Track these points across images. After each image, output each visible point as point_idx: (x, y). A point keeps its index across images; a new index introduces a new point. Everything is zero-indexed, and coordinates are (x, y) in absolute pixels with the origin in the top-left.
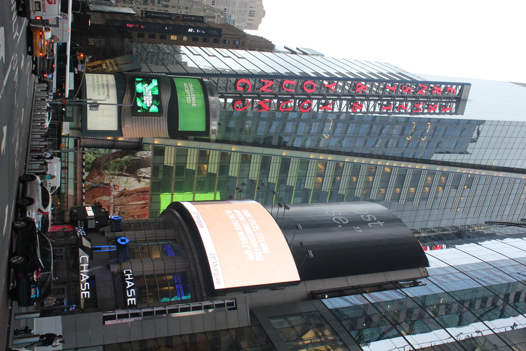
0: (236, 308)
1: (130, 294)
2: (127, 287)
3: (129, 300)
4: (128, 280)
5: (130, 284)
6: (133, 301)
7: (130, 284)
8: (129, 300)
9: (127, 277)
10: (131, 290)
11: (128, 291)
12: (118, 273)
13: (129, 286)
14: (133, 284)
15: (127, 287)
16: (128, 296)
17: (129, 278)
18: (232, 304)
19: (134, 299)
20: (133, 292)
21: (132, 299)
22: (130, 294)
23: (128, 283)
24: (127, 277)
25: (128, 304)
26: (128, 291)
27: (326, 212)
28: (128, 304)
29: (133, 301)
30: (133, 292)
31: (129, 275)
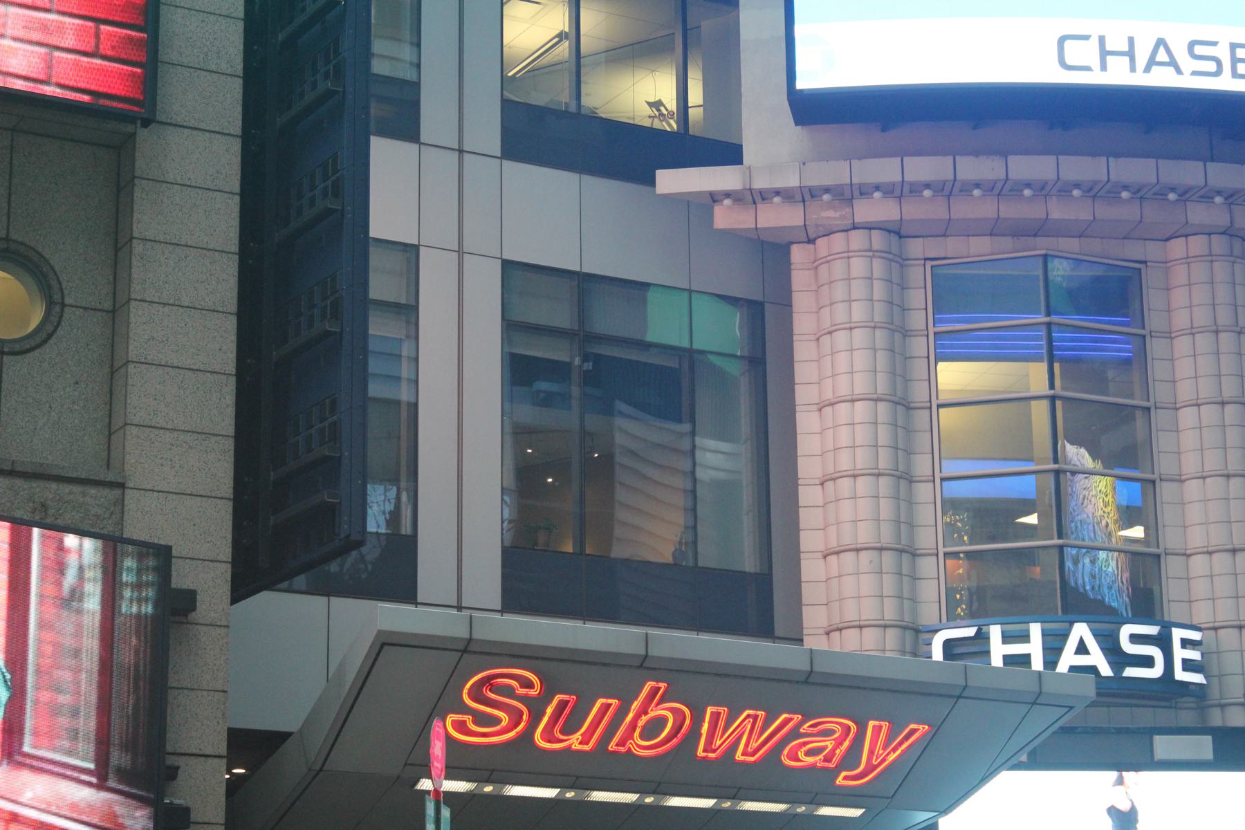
1: (1148, 662)
2: (1106, 670)
3: (1180, 675)
4: (1051, 663)
5: (1082, 649)
6: (1185, 643)
7: (1082, 649)
11: (1131, 672)
13: (1097, 658)
15: (1106, 670)
16: (1157, 672)
17: (1034, 648)
19: (1178, 634)
20: (1135, 639)
21: (1179, 654)
22: (1148, 662)
23: (1068, 659)
25: (1197, 678)
26: (1131, 672)
28: (1197, 678)
29: (1185, 643)
30: (1135, 639)
31: (999, 650)
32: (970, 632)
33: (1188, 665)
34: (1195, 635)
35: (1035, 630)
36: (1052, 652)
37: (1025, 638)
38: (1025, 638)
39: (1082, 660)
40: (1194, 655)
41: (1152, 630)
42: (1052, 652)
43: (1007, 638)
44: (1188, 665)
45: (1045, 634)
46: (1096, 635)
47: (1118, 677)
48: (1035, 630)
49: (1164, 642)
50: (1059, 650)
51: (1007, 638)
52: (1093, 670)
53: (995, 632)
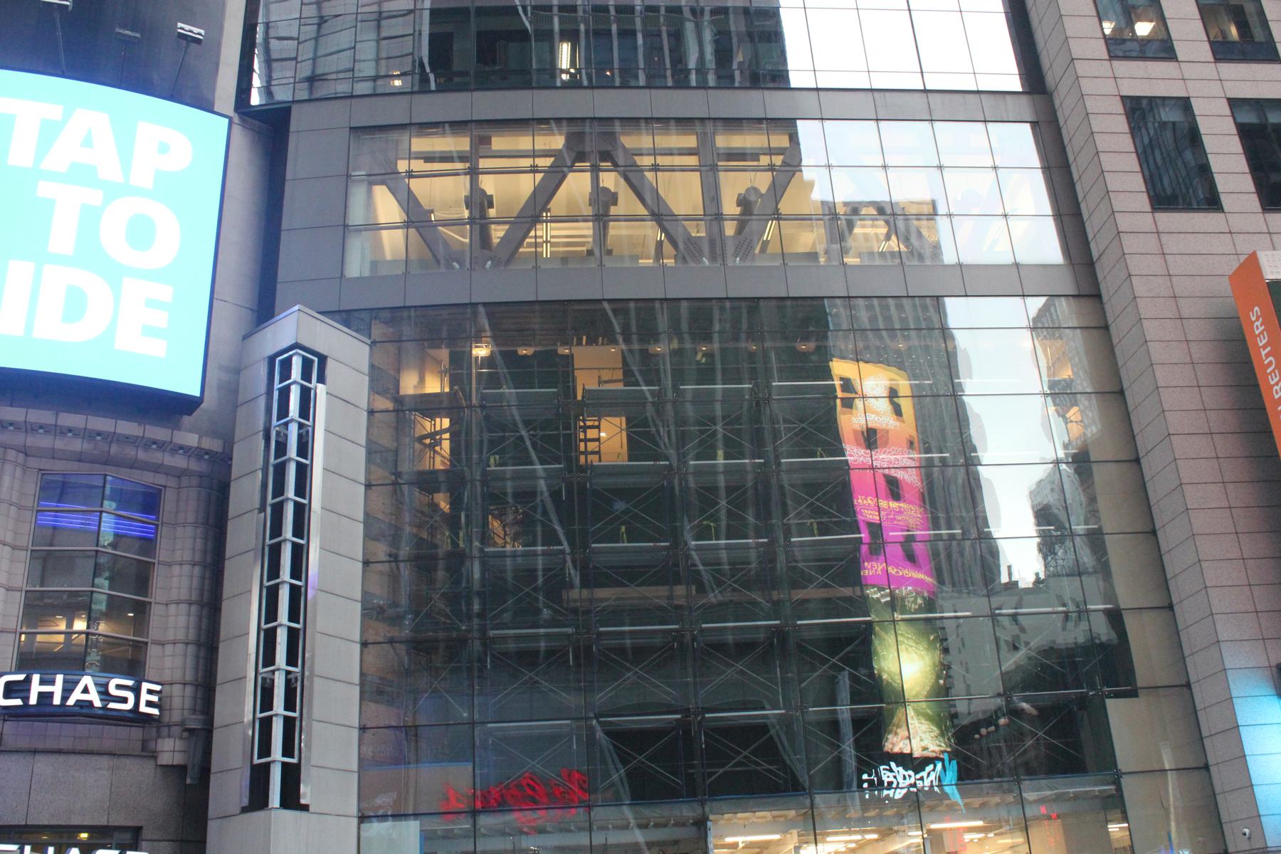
0: (323, 359)
1: (125, 700)
2: (97, 703)
3: (143, 708)
4: (65, 698)
5: (86, 690)
6: (150, 692)
7: (86, 690)
9: (45, 697)
10: (113, 691)
11: (112, 705)
14: (87, 680)
16: (129, 705)
17: (57, 689)
18: (307, 365)
19: (145, 686)
20: (119, 687)
21: (145, 697)
22: (125, 700)
24: (45, 697)
25: (155, 711)
26: (112, 705)
28: (155, 711)
29: (150, 692)
30: (119, 687)
31: (36, 688)
32: (21, 677)
33: (149, 704)
34: (158, 688)
35: (59, 678)
36: (67, 692)
37: (52, 682)
38: (52, 682)
39: (85, 697)
40: (155, 698)
41: (130, 683)
42: (67, 692)
43: (42, 682)
44: (149, 704)
45: (65, 682)
46: (96, 684)
47: (104, 708)
48: (59, 678)
49: (137, 691)
50: (72, 691)
51: (42, 682)
52: (91, 703)
53: (36, 678)
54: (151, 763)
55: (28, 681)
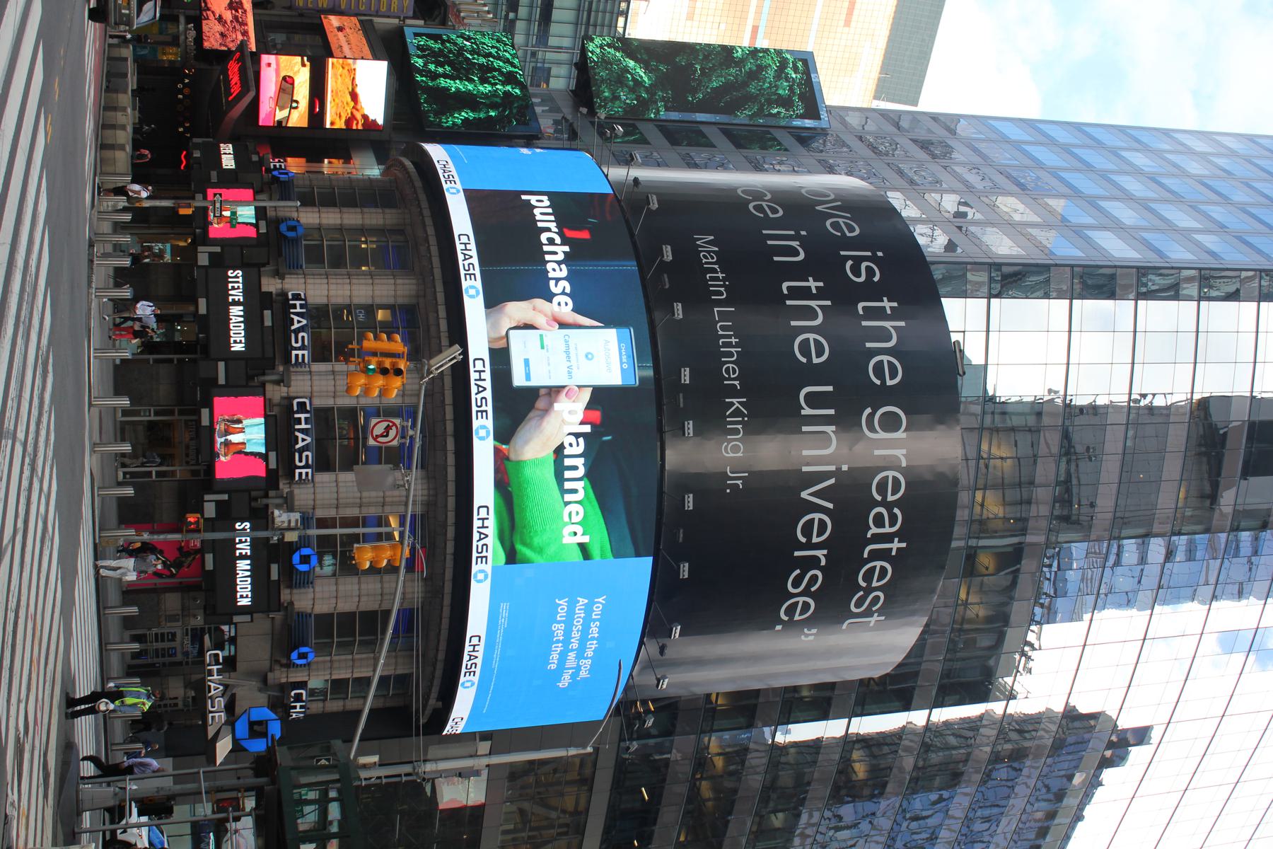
1: (300, 461)
3: (297, 471)
4: (299, 430)
5: (303, 440)
7: (303, 440)
8: (297, 471)
9: (299, 421)
12: (278, 295)
13: (301, 444)
16: (298, 464)
17: (303, 426)
19: (309, 471)
21: (304, 471)
23: (300, 436)
24: (299, 421)
27: (803, 191)
31: (303, 416)
33: (300, 474)
44: (300, 474)
54: (267, 664)
55: (307, 412)
